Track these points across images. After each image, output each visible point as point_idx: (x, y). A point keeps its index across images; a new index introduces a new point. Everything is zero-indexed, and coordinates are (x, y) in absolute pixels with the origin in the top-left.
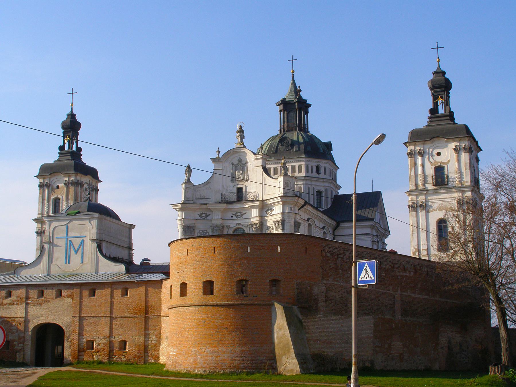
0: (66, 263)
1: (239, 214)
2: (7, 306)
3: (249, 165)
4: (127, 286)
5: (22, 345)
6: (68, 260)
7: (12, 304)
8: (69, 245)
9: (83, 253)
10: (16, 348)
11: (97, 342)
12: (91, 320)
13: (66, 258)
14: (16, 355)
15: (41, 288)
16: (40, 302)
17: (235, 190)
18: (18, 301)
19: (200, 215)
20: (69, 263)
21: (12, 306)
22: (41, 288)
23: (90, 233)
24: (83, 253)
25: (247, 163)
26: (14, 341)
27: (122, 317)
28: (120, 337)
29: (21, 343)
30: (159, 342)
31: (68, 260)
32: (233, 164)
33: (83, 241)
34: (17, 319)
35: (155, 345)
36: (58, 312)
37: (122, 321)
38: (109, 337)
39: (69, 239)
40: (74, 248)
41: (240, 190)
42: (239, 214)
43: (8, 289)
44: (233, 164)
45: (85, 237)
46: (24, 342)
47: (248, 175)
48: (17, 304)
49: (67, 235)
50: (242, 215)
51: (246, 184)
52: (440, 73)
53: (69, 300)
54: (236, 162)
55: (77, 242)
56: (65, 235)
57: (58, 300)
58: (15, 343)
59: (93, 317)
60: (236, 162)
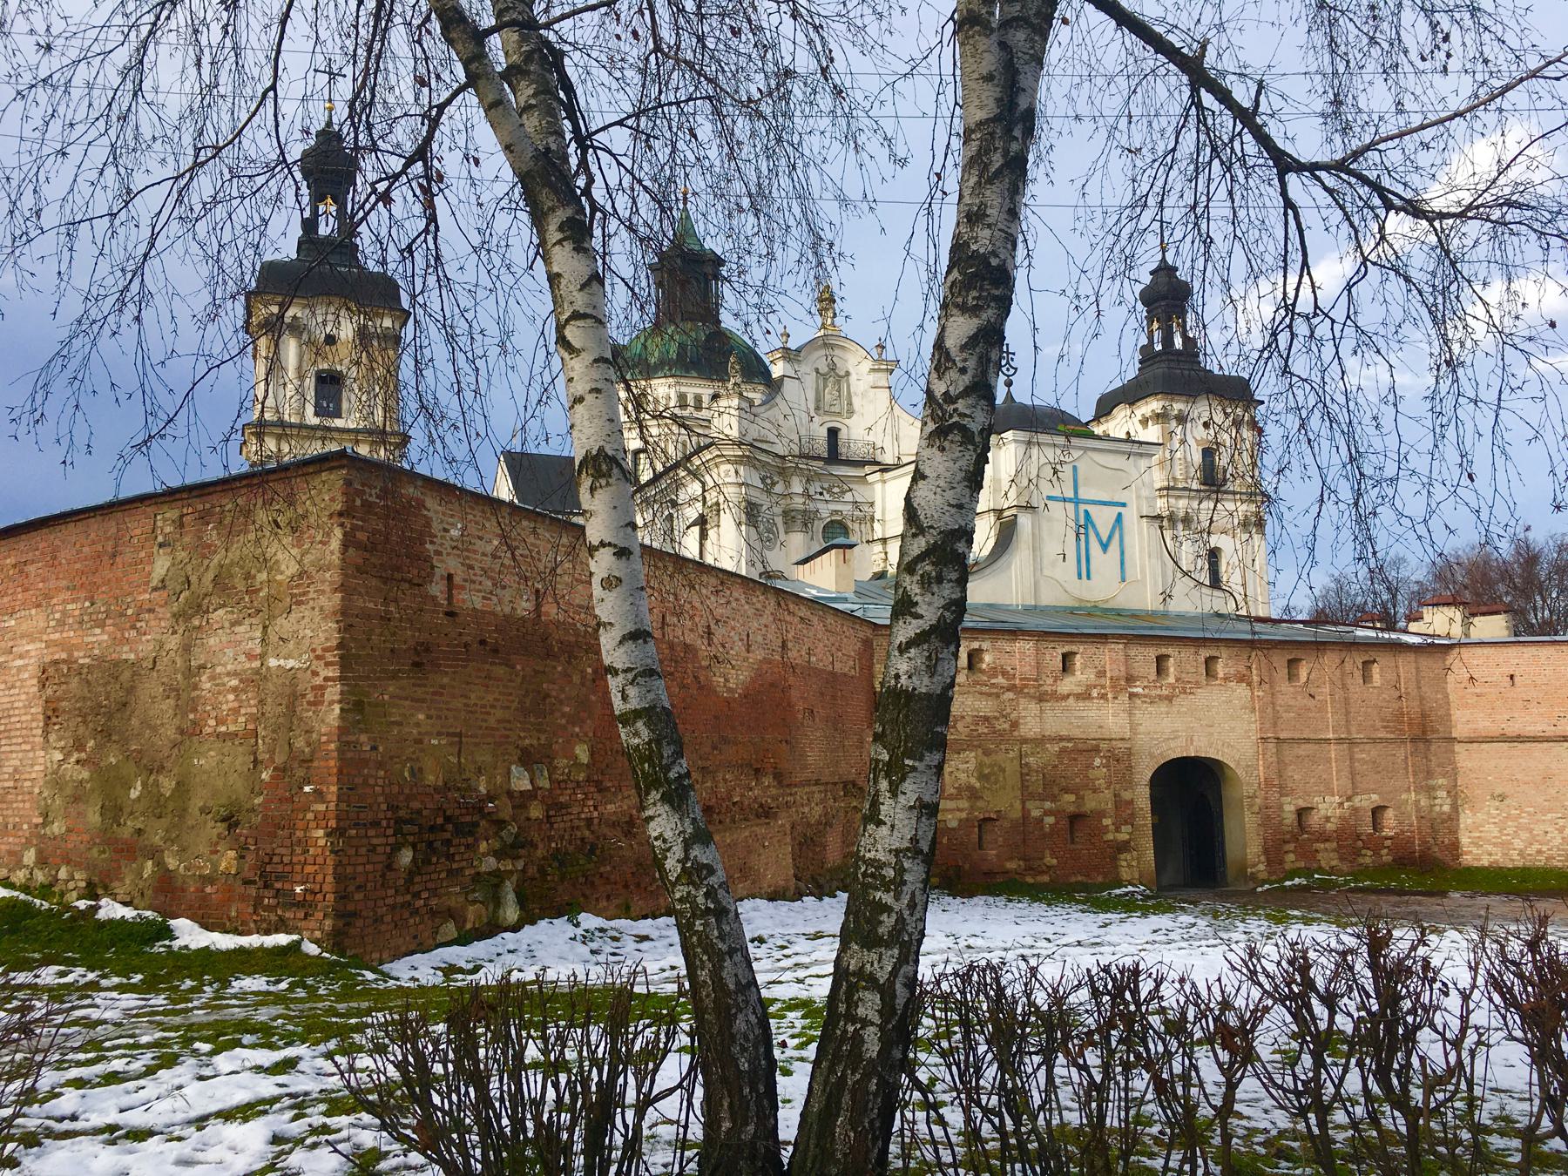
0: (1080, 577)
1: (836, 490)
2: (1071, 700)
3: (853, 378)
4: (1372, 655)
5: (1128, 828)
6: (1084, 570)
7: (1085, 696)
8: (1084, 527)
9: (1122, 553)
10: (1110, 836)
11: (1323, 812)
12: (1304, 750)
13: (1079, 561)
14: (1115, 859)
15: (1164, 651)
16: (1165, 692)
17: (823, 432)
18: (1103, 687)
19: (763, 480)
20: (1088, 577)
21: (1087, 703)
22: (1164, 651)
23: (1138, 497)
24: (1122, 553)
25: (848, 374)
26: (1101, 814)
27: (1374, 741)
28: (1375, 797)
29: (1126, 823)
30: (1455, 808)
31: (1084, 570)
32: (817, 371)
33: (1120, 515)
34: (1104, 745)
35: (1450, 818)
36: (1213, 720)
37: (1374, 753)
38: (1349, 799)
39: (1082, 507)
40: (1097, 535)
41: (833, 433)
42: (836, 490)
43: (1067, 649)
44: (817, 371)
45: (1124, 505)
46: (1133, 815)
47: (850, 404)
48: (1103, 697)
49: (1076, 493)
50: (843, 492)
51: (847, 421)
52: (1165, 271)
53: (1242, 690)
54: (824, 369)
55: (1103, 519)
56: (1070, 494)
57: (1216, 690)
58: (1107, 822)
59: (1308, 740)
60: (824, 369)
